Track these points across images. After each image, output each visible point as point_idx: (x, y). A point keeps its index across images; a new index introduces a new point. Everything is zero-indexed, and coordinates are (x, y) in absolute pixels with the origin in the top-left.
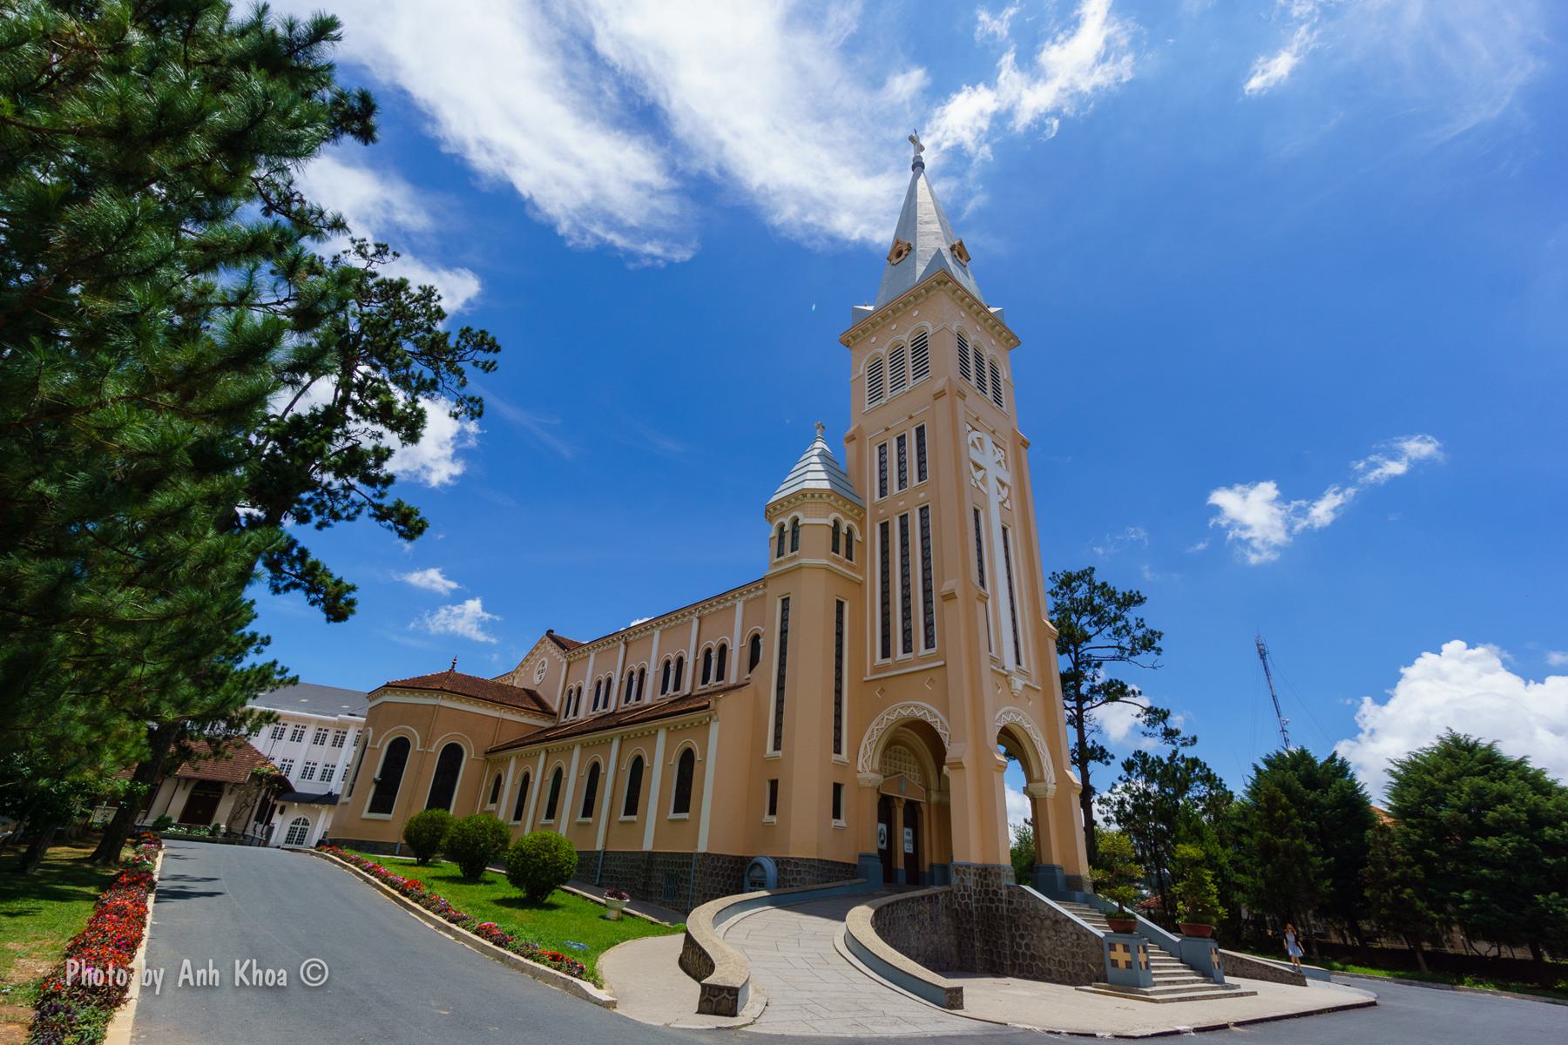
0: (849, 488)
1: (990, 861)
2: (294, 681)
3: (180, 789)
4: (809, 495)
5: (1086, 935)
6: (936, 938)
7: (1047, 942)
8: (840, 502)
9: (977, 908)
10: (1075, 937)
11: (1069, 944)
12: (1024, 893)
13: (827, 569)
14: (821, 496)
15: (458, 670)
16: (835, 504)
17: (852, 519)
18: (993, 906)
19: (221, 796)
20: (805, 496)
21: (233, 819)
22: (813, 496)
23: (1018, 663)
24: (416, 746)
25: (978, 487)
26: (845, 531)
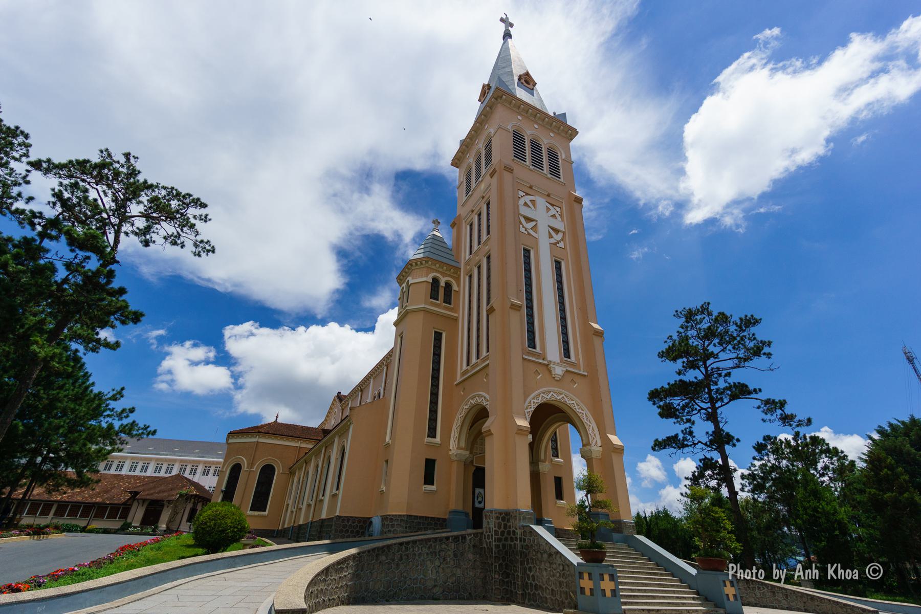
0: (451, 258)
1: (511, 507)
2: (154, 432)
3: (140, 506)
4: (414, 264)
12: (533, 532)
15: (279, 421)
17: (449, 276)
18: (512, 543)
19: (163, 508)
21: (169, 522)
24: (245, 468)
26: (444, 285)
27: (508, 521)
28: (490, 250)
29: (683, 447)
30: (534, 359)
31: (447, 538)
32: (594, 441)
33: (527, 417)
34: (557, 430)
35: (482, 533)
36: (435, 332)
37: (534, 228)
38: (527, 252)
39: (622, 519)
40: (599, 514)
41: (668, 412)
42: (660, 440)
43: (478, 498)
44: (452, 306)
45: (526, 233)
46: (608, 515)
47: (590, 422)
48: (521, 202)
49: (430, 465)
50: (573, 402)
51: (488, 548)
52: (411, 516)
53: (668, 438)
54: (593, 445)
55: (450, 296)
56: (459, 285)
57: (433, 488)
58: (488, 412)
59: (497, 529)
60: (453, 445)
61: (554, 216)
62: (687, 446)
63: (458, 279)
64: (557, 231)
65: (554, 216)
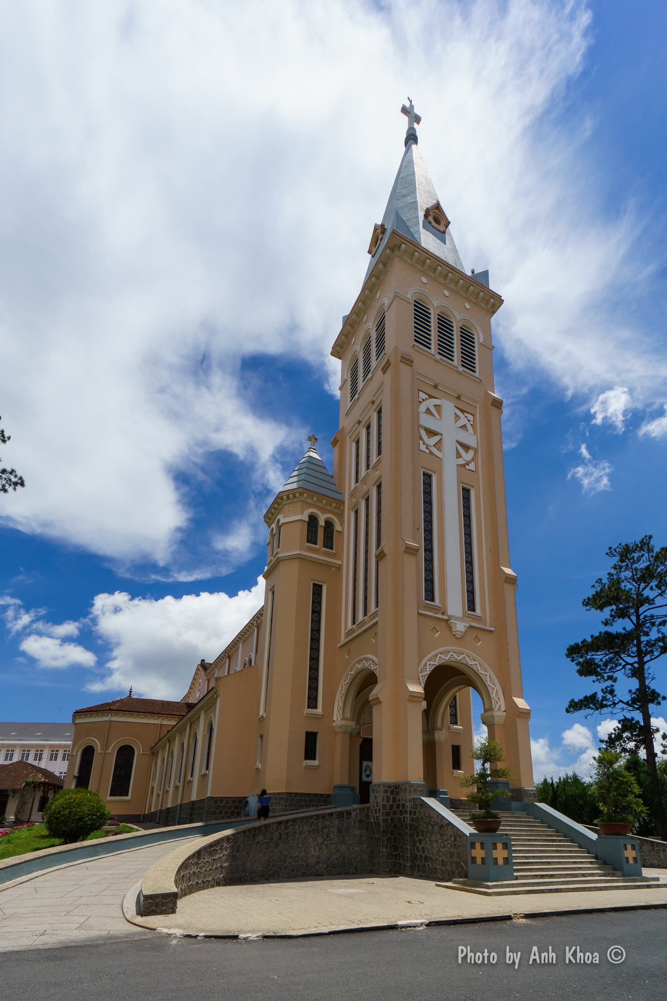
1: (400, 779)
5: (460, 837)
6: (343, 848)
7: (435, 845)
8: (315, 498)
9: (385, 820)
10: (453, 839)
11: (449, 846)
13: (300, 558)
14: (294, 496)
16: (310, 501)
18: (402, 817)
20: (282, 499)
22: (288, 497)
23: (471, 606)
24: (98, 750)
25: (431, 453)
27: (398, 794)
28: (380, 477)
29: (601, 708)
30: (431, 614)
31: (331, 815)
32: (498, 706)
33: (422, 682)
34: (458, 694)
35: (369, 808)
36: (314, 584)
37: (438, 445)
38: (428, 477)
39: (523, 787)
40: (498, 783)
41: (588, 669)
42: (576, 700)
43: (366, 771)
44: (334, 551)
45: (428, 451)
46: (508, 784)
47: (494, 684)
48: (423, 408)
49: (311, 739)
50: (476, 662)
51: (375, 822)
52: (290, 793)
53: (586, 697)
54: (496, 710)
55: (331, 538)
56: (342, 524)
57: (316, 763)
58: (377, 678)
59: (385, 803)
60: (337, 716)
61: (464, 427)
62: (606, 706)
63: (341, 516)
64: (466, 448)
65: (464, 427)
